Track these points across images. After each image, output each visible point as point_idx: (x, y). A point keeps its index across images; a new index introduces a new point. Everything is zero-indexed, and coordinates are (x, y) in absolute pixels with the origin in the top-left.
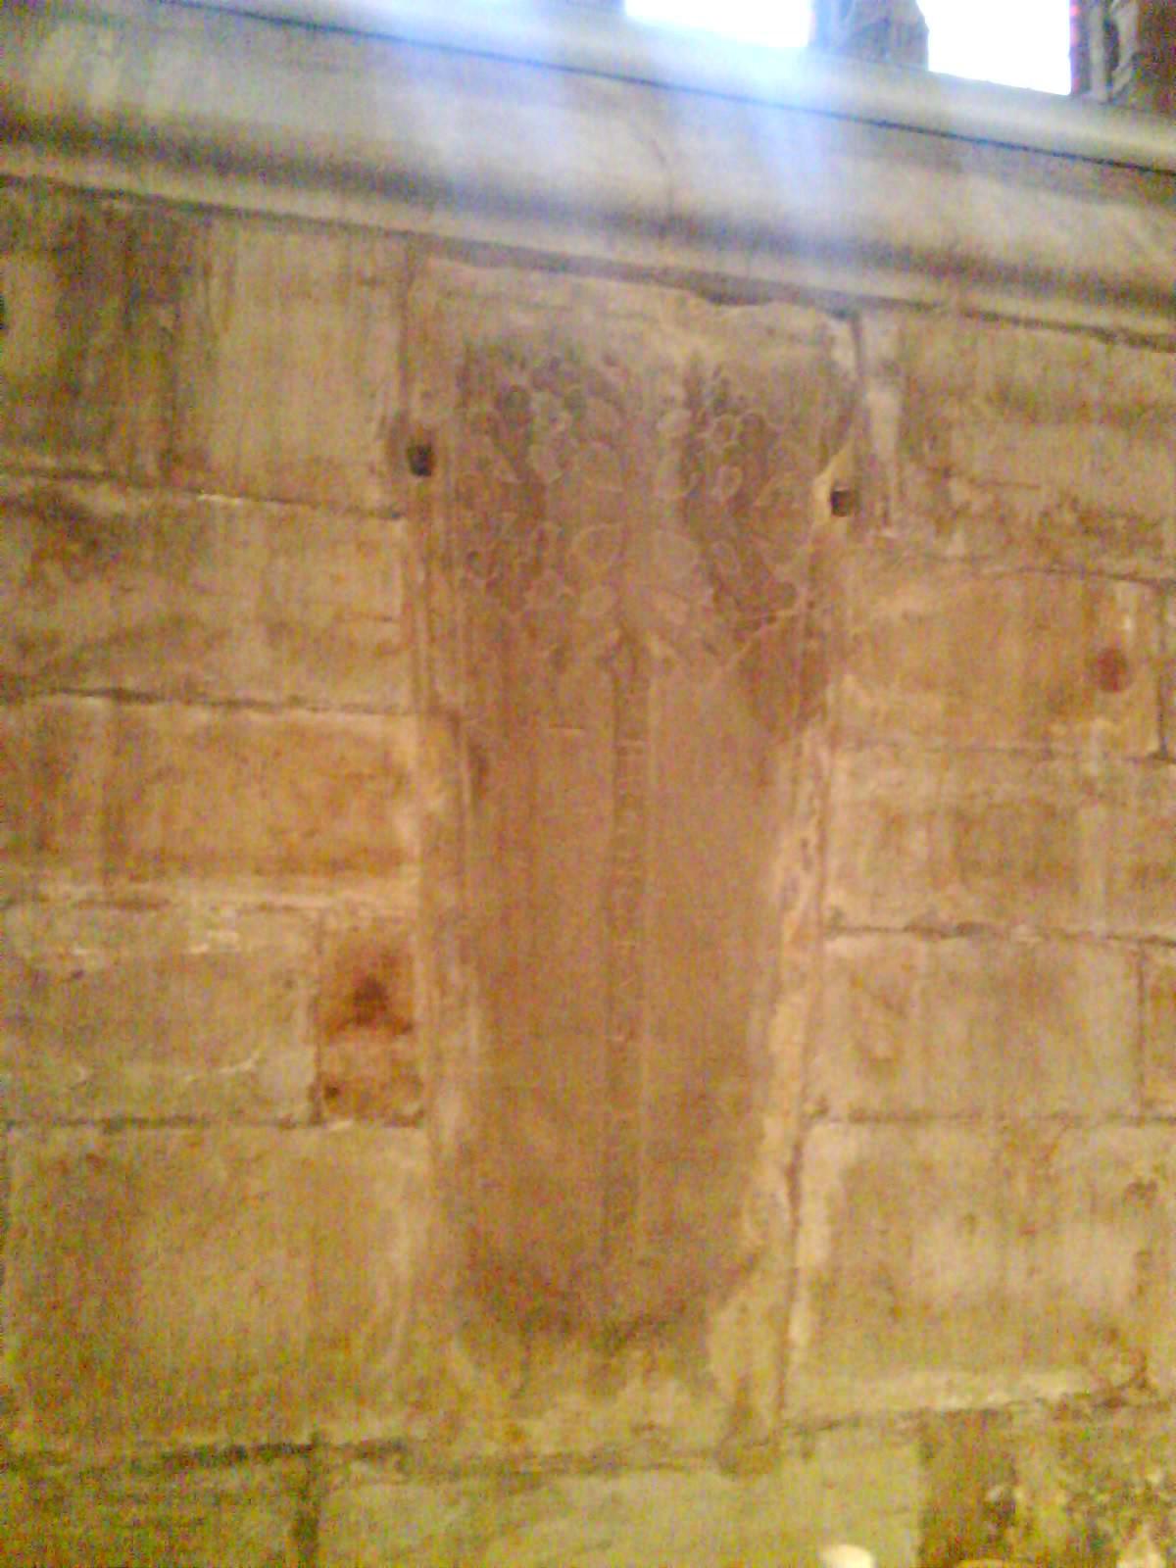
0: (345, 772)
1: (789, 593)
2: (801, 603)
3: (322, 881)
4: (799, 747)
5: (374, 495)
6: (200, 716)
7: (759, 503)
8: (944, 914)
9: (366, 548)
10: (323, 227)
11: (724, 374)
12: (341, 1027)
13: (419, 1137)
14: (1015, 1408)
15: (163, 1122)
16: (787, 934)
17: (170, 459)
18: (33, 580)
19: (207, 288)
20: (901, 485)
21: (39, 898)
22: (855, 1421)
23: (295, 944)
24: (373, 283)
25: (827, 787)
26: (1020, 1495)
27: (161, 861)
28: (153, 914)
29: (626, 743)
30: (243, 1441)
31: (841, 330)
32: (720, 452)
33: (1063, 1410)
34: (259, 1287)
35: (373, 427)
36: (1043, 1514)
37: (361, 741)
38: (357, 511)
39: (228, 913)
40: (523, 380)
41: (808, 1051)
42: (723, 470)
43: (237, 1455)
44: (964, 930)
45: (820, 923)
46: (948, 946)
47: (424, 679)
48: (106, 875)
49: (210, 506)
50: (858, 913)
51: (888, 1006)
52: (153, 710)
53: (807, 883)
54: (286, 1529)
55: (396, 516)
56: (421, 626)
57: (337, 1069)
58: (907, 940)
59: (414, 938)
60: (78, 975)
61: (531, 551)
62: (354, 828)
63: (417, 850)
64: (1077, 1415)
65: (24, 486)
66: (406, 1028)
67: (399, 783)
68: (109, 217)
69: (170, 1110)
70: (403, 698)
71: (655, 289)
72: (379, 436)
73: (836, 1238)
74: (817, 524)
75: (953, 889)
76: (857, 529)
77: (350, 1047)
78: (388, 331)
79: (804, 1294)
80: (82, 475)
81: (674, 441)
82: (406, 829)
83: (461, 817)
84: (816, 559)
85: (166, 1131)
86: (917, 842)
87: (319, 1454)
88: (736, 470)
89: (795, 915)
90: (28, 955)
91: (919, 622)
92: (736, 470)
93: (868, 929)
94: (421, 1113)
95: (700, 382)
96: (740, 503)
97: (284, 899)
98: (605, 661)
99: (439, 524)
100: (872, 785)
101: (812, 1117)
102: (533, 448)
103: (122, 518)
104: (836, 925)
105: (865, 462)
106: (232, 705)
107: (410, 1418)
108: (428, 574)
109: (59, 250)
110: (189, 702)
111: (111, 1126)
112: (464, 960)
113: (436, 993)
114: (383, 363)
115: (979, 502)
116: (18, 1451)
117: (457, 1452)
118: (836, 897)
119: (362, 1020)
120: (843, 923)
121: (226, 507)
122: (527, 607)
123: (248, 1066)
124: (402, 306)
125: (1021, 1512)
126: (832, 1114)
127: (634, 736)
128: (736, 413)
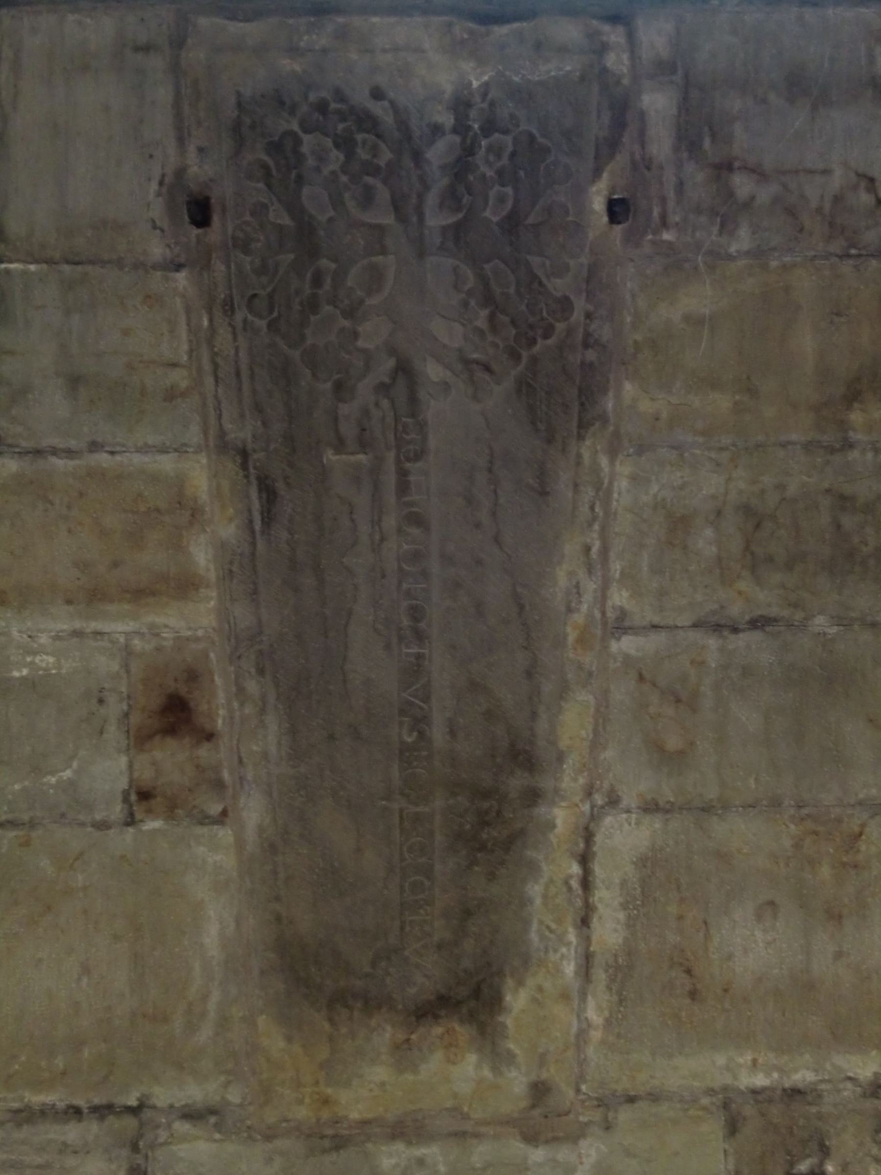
0: (143, 509)
1: (566, 305)
2: (577, 316)
4: (579, 456)
5: (157, 250)
7: (530, 220)
8: (736, 610)
12: (150, 737)
13: (225, 834)
16: (572, 636)
20: (680, 187)
22: (655, 1097)
24: (146, 49)
25: (609, 492)
29: (408, 465)
30: (80, 1102)
31: (615, 35)
34: (86, 969)
35: (154, 186)
39: (44, 639)
40: (295, 127)
41: (596, 744)
42: (493, 193)
43: (76, 1112)
44: (758, 623)
45: (605, 623)
46: (740, 641)
47: (212, 420)
49: (7, 272)
53: (591, 587)
55: (179, 267)
56: (207, 366)
57: (145, 775)
58: (694, 635)
61: (308, 290)
63: (212, 576)
66: (210, 736)
67: (193, 515)
70: (194, 434)
71: (419, 19)
72: (159, 194)
73: (630, 924)
76: (632, 239)
77: (158, 755)
78: (163, 94)
79: (600, 976)
81: (443, 168)
84: (593, 271)
87: (147, 1114)
88: (509, 190)
89: (579, 618)
92: (509, 190)
93: (655, 627)
94: (224, 813)
95: (469, 105)
97: (94, 625)
98: (383, 389)
99: (219, 267)
101: (602, 807)
102: (306, 191)
107: (228, 1084)
108: (211, 320)
112: (261, 672)
113: (236, 705)
115: (765, 195)
117: (271, 1116)
118: (619, 597)
119: (171, 731)
121: (24, 273)
122: (309, 342)
123: (67, 774)
124: (175, 69)
126: (624, 804)
127: (418, 456)
128: (506, 132)
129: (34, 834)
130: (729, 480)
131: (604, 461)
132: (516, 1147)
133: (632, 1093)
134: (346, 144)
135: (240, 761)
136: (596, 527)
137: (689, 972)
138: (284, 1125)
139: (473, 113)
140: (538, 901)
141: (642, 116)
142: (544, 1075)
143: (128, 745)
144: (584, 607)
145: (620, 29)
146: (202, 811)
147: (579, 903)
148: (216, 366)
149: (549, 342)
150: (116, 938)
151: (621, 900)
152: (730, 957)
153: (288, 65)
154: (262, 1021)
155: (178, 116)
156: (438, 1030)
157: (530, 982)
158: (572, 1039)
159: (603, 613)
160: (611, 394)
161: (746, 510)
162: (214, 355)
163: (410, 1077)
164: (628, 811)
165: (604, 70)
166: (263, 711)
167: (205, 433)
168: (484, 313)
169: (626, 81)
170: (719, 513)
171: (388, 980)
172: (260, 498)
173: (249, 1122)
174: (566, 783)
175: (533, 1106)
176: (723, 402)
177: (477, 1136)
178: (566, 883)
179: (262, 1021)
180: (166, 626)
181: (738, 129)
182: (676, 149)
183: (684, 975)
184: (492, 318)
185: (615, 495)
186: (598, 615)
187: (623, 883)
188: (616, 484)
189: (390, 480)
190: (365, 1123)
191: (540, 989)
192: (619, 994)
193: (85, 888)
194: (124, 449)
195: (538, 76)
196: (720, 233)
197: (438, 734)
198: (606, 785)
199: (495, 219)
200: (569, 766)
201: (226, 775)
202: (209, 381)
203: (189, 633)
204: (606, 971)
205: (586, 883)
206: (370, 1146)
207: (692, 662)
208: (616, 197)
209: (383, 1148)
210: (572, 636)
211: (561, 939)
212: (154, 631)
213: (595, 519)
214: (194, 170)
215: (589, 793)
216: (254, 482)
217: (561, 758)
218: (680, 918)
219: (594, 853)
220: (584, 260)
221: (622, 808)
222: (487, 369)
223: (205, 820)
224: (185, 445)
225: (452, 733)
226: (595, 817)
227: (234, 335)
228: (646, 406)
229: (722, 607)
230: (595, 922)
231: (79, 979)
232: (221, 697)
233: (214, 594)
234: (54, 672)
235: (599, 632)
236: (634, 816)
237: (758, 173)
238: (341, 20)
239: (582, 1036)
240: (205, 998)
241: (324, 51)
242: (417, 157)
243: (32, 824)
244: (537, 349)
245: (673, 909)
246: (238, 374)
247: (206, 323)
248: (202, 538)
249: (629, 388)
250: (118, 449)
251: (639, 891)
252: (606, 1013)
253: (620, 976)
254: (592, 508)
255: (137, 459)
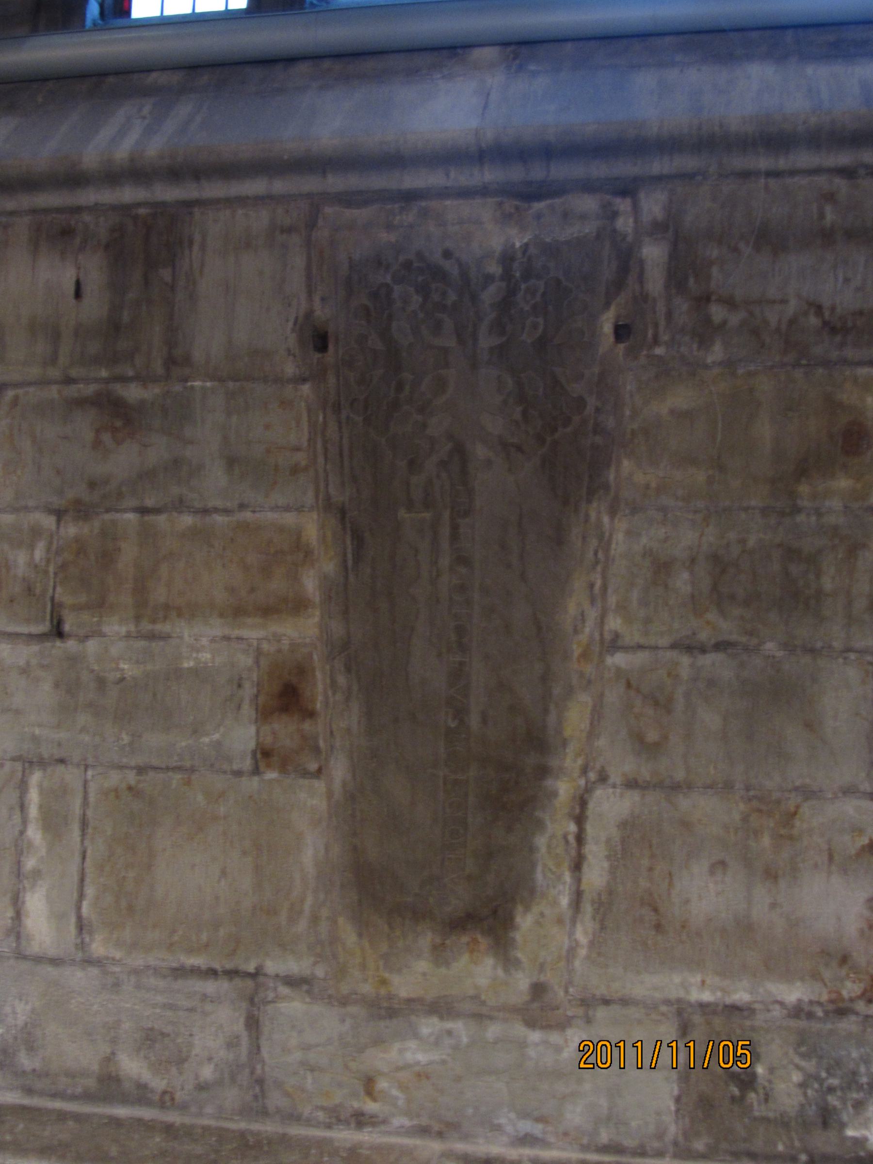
0: (272, 550)
1: (581, 403)
2: (589, 409)
3: (258, 620)
4: (587, 516)
6: (187, 520)
8: (704, 636)
9: (285, 404)
10: (259, 200)
11: (533, 250)
13: (320, 785)
14: (757, 1006)
15: (168, 769)
16: (577, 651)
17: (171, 362)
18: (97, 444)
19: (191, 251)
20: (669, 315)
21: (102, 635)
22: (625, 1002)
23: (245, 661)
24: (289, 230)
26: (760, 1070)
27: (168, 610)
28: (161, 643)
30: (217, 966)
31: (623, 205)
32: (527, 308)
33: (798, 1011)
34: (224, 873)
35: (290, 324)
36: (780, 1087)
37: (281, 529)
38: (279, 380)
39: (204, 641)
40: (388, 279)
41: (592, 734)
43: (212, 973)
44: (721, 646)
46: (707, 660)
48: (138, 618)
49: (192, 387)
50: (632, 635)
51: (656, 704)
52: (162, 518)
53: (592, 614)
54: (242, 1020)
55: (304, 380)
57: (269, 740)
58: (670, 654)
59: (315, 657)
60: (123, 679)
62: (278, 585)
63: (317, 600)
64: (810, 1015)
65: (90, 390)
66: (311, 714)
67: (306, 556)
68: (135, 218)
69: (174, 762)
70: (309, 498)
71: (478, 201)
72: (293, 330)
73: (613, 871)
74: (601, 351)
75: (712, 616)
77: (276, 726)
78: (298, 261)
79: (588, 908)
80: (123, 379)
82: (310, 584)
83: (346, 578)
85: (170, 774)
86: (682, 581)
87: (261, 979)
89: (584, 638)
90: (96, 668)
91: (684, 416)
92: (541, 320)
93: (640, 647)
94: (320, 770)
96: (542, 344)
97: (236, 633)
99: (332, 380)
100: (644, 540)
101: (594, 783)
102: (394, 324)
103: (143, 402)
104: (614, 644)
105: (642, 299)
106: (206, 511)
107: (315, 964)
108: (324, 418)
109: (107, 247)
110: (180, 512)
111: (141, 770)
112: (348, 669)
113: (330, 693)
114: (296, 282)
115: (735, 319)
116: (95, 955)
117: (345, 989)
118: (614, 623)
120: (620, 643)
121: (203, 388)
123: (216, 736)
124: (308, 243)
125: (761, 1081)
126: (611, 781)
129: (193, 777)
130: (701, 536)
131: (606, 519)
132: (519, 1029)
133: (608, 998)
134: (424, 290)
135: (332, 732)
136: (599, 568)
137: (656, 910)
138: (354, 996)
139: (516, 265)
140: (543, 850)
141: (641, 263)
142: (542, 978)
143: (257, 718)
144: (587, 630)
145: (628, 201)
146: (305, 769)
147: (573, 853)
148: (326, 450)
149: (569, 430)
150: (244, 853)
151: (606, 853)
152: (687, 901)
153: (385, 237)
154: (341, 920)
155: (309, 277)
156: (465, 939)
157: (536, 909)
158: (564, 953)
159: (601, 635)
160: (612, 470)
161: (715, 558)
162: (325, 442)
163: (443, 970)
164: (614, 786)
165: (614, 231)
166: (347, 699)
167: (317, 497)
168: (519, 409)
169: (630, 239)
170: (693, 560)
171: (431, 900)
172: (352, 544)
173: (330, 992)
174: (568, 762)
175: (533, 1000)
176: (700, 476)
177: (491, 1018)
178: (565, 837)
179: (341, 920)
180: (285, 635)
181: (715, 271)
182: (667, 287)
183: (652, 913)
184: (524, 413)
185: (613, 546)
186: (597, 636)
187: (608, 841)
188: (614, 536)
189: (445, 531)
190: (409, 1001)
191: (542, 915)
192: (602, 922)
193: (225, 818)
194: (262, 509)
195: (564, 238)
196: (699, 348)
197: (474, 721)
198: (598, 766)
199: (529, 341)
200: (571, 749)
201: (322, 744)
202: (321, 460)
203: (300, 641)
204: (592, 905)
205: (580, 839)
206: (413, 1018)
207: (669, 674)
208: (620, 323)
209: (423, 1020)
210: (577, 650)
211: (559, 878)
212: (277, 638)
213: (597, 562)
214: (318, 313)
215: (584, 770)
216: (349, 532)
217: (565, 743)
218: (651, 869)
219: (587, 817)
220: (596, 370)
221: (609, 785)
222: (519, 449)
223: (306, 774)
224: (303, 507)
225: (484, 721)
226: (589, 789)
227: (340, 428)
228: (639, 478)
229: (694, 634)
230: (585, 868)
231: (219, 881)
232: (320, 687)
233: (317, 613)
234: (210, 665)
235: (597, 648)
236: (618, 790)
237: (730, 303)
238: (423, 204)
239: (572, 951)
240: (302, 901)
241: (411, 226)
242: (474, 298)
243: (192, 770)
244: (557, 436)
245: (645, 862)
246: (341, 455)
247: (321, 418)
248: (312, 573)
249: (627, 465)
250: (258, 509)
251: (619, 848)
252: (591, 936)
253: (602, 909)
254: (596, 553)
255: (270, 515)
